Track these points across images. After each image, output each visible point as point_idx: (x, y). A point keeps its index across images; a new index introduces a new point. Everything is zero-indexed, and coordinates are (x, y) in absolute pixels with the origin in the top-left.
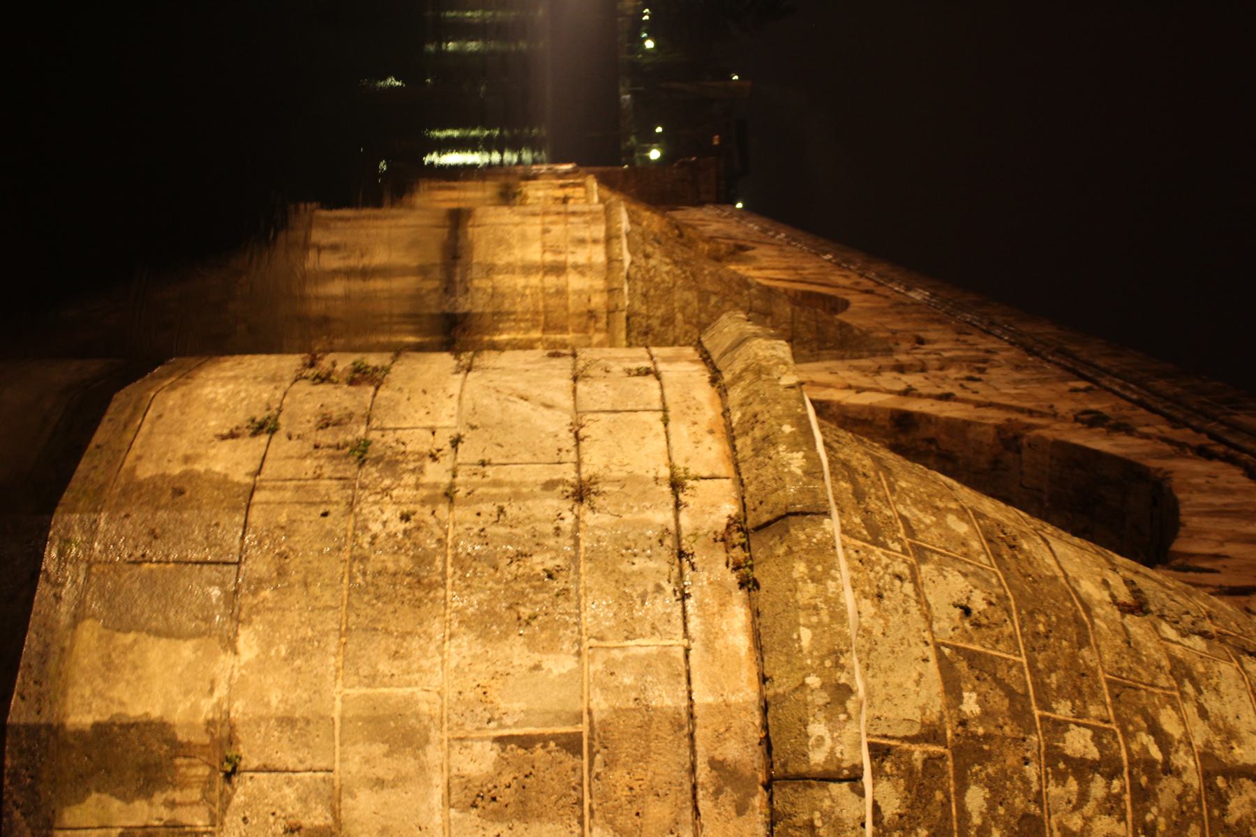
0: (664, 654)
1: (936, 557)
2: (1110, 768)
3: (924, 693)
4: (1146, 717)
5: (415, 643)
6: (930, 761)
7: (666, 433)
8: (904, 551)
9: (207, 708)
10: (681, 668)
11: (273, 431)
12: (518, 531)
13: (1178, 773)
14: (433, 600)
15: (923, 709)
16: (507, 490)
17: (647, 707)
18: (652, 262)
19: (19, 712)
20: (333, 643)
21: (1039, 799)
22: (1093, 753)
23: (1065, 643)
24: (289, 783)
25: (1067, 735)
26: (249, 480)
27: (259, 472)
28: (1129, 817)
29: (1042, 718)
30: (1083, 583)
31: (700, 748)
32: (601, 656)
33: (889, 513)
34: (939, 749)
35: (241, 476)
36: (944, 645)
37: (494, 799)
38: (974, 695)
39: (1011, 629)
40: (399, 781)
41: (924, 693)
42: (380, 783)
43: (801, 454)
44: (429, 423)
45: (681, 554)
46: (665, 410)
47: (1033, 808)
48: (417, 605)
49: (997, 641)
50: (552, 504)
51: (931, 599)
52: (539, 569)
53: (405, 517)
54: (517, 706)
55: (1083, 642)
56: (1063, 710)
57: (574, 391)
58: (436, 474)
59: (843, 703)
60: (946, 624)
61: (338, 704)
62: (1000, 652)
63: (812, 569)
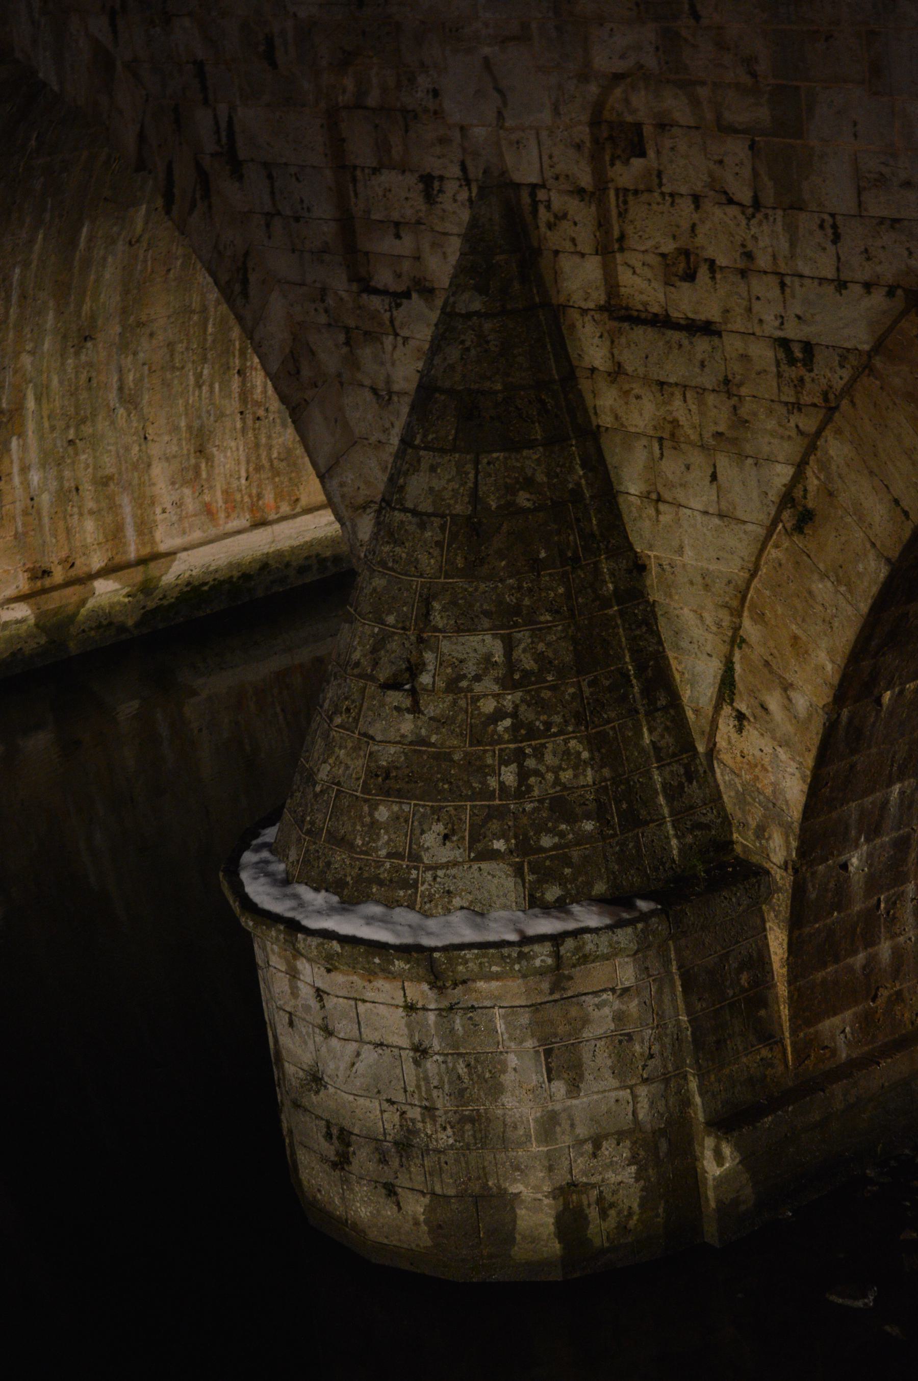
0: (504, 1017)
1: (414, 846)
3: (498, 873)
4: (485, 724)
5: (508, 1120)
6: (532, 871)
7: (374, 1002)
8: (417, 868)
9: (546, 1201)
10: (510, 1010)
11: (393, 1186)
12: (446, 1080)
13: (516, 707)
14: (486, 1114)
15: (508, 876)
16: (422, 1083)
19: (556, 1275)
20: (511, 1154)
21: (541, 801)
22: (513, 767)
23: (452, 772)
24: (575, 1161)
25: (507, 783)
26: (428, 1196)
27: (422, 1192)
28: (543, 741)
29: (500, 800)
30: (402, 731)
31: (546, 999)
32: (507, 1043)
33: (388, 865)
34: (526, 864)
35: (426, 1200)
36: (469, 856)
38: (495, 841)
39: (451, 808)
40: (571, 1118)
41: (498, 873)
42: (572, 1126)
43: (396, 962)
45: (451, 1008)
46: (356, 999)
48: (489, 1120)
49: (461, 819)
50: (430, 1065)
51: (444, 860)
52: (465, 1070)
53: (445, 1129)
54: (534, 1077)
55: (448, 757)
56: (493, 783)
58: (414, 1113)
59: (526, 954)
60: (457, 852)
61: (540, 1149)
63: (461, 964)
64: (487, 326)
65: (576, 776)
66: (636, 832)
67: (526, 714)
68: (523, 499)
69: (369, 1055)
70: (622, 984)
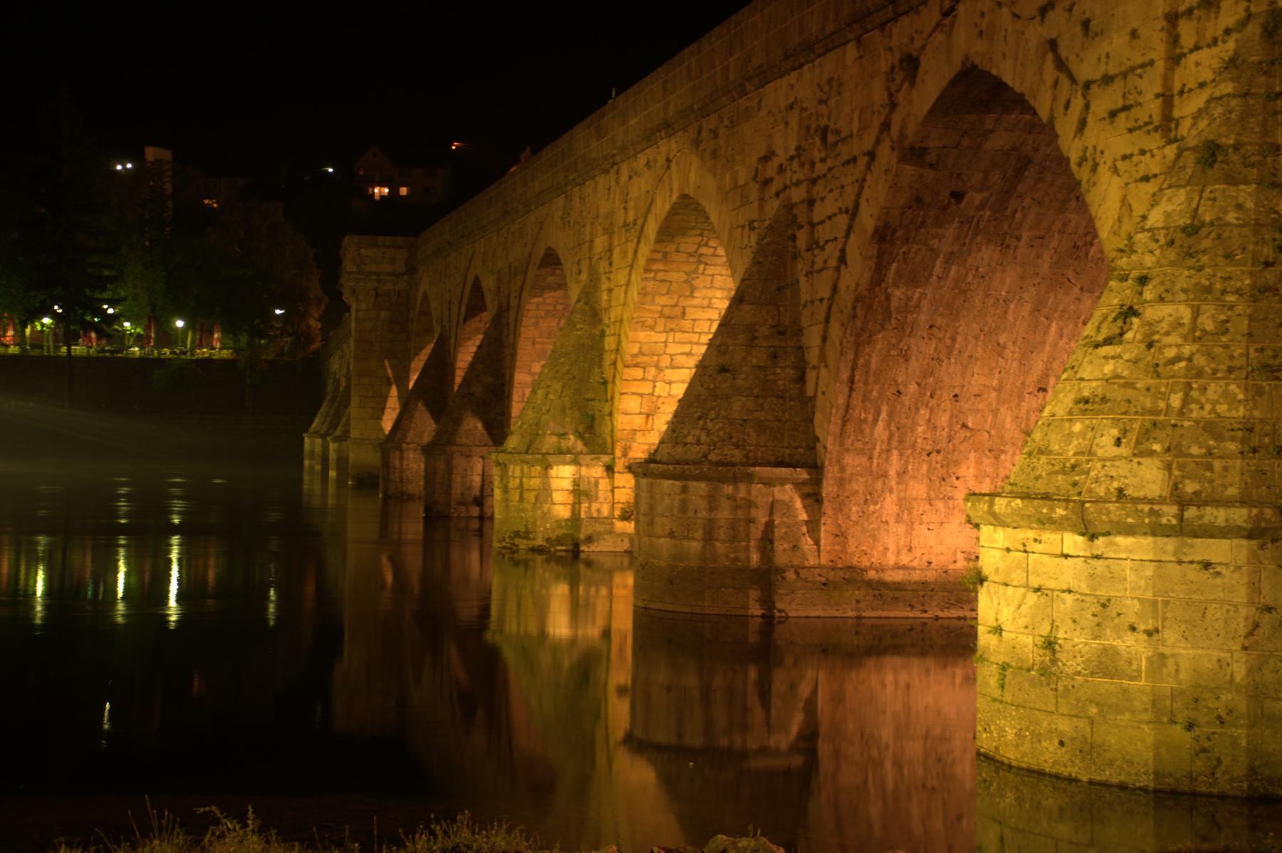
2: (1188, 386)
13: (1192, 354)
17: (1153, 576)
18: (703, 438)
21: (1197, 422)
28: (1207, 381)
29: (1165, 416)
30: (1106, 372)
31: (1169, 559)
37: (1184, 632)
40: (1177, 664)
42: (1177, 671)
44: (1031, 646)
47: (1201, 425)
54: (1150, 621)
56: (1162, 405)
57: (1016, 587)
62: (1136, 426)
64: (1234, 102)
65: (1229, 410)
66: (1273, 460)
67: (1200, 360)
68: (1231, 217)
69: (1032, 598)
70: (1236, 562)
